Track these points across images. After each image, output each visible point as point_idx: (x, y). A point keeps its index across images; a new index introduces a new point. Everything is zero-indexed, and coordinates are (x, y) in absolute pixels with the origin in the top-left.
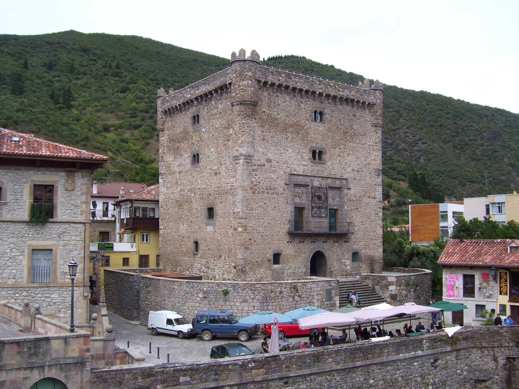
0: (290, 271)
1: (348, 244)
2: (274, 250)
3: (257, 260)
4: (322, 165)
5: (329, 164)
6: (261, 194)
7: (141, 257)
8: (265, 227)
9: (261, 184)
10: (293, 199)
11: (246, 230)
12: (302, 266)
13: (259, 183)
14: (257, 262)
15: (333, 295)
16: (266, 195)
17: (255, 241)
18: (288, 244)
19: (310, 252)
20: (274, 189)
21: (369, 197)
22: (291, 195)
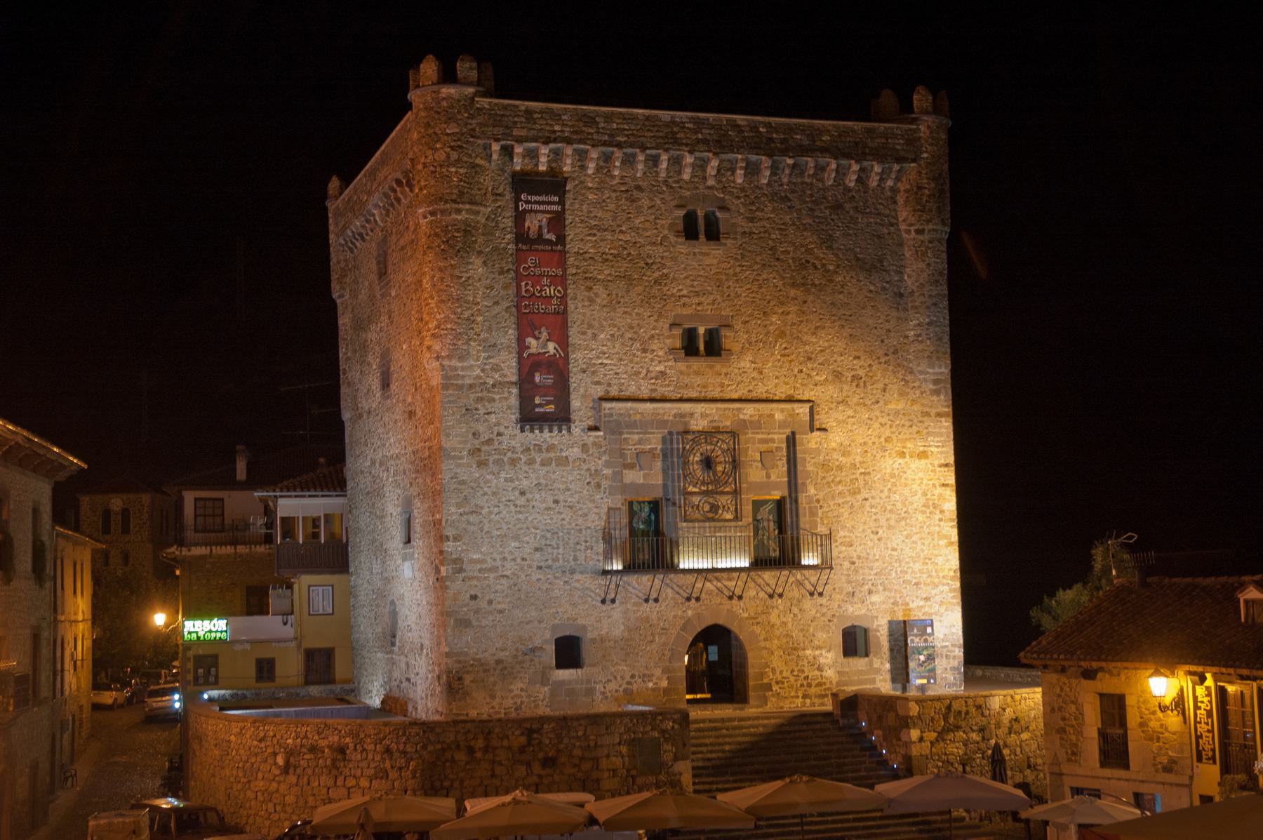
0: (612, 686)
1: (823, 600)
2: (554, 628)
3: (501, 655)
4: (718, 367)
5: (745, 363)
6: (507, 467)
7: (310, 655)
8: (523, 559)
9: (504, 439)
10: (618, 476)
11: (461, 570)
12: (658, 672)
13: (499, 434)
14: (498, 662)
15: (667, 757)
16: (526, 468)
17: (490, 602)
18: (604, 607)
19: (684, 628)
20: (551, 448)
21: (902, 455)
22: (608, 464)
